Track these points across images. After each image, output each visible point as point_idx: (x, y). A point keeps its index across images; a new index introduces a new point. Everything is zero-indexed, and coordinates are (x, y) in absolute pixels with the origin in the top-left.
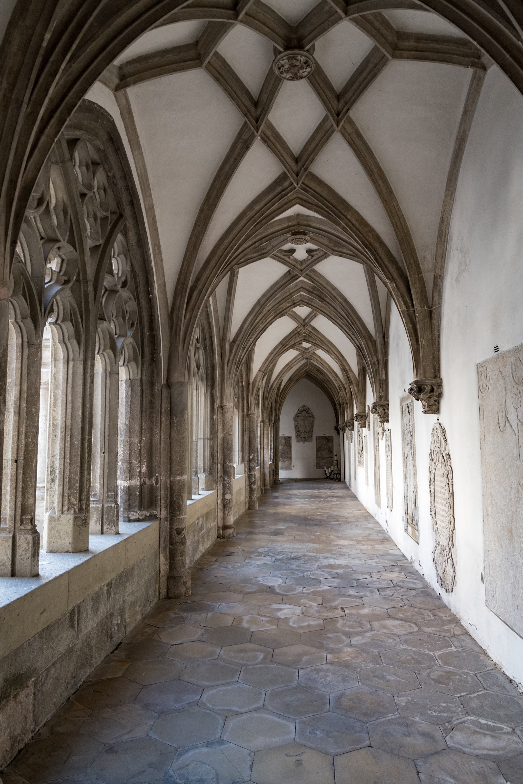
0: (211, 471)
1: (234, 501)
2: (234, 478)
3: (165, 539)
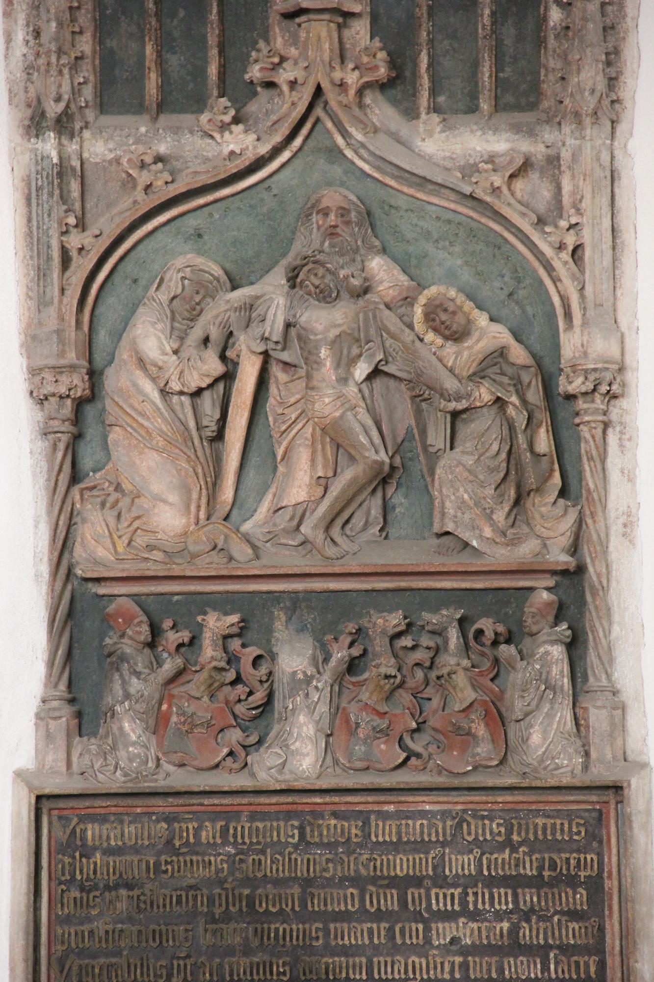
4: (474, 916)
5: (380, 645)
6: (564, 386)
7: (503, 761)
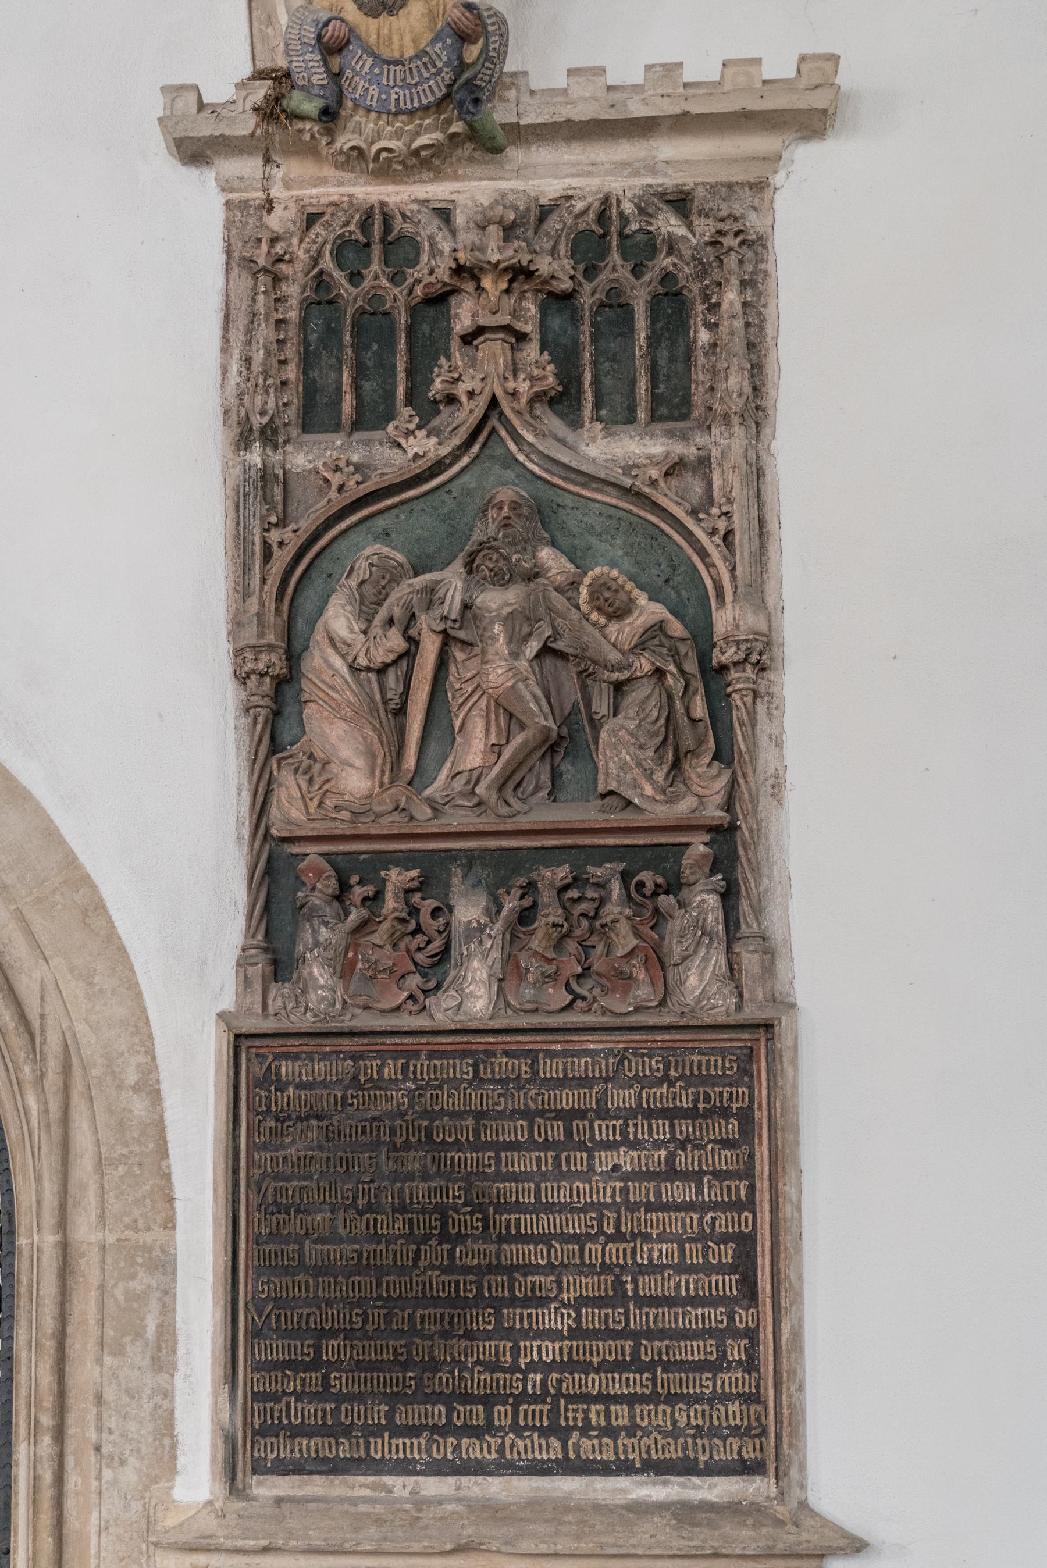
4: (635, 1145)
5: (547, 896)
6: (718, 657)
7: (663, 1003)
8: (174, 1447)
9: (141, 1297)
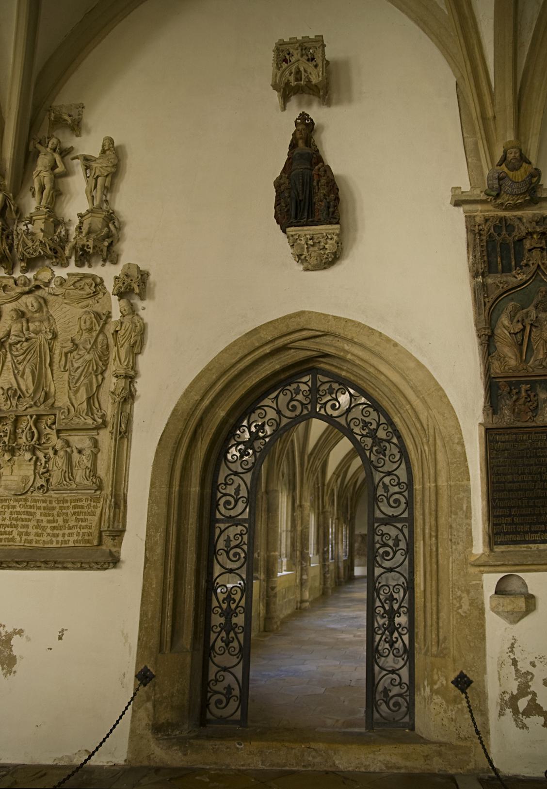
0: (291, 557)
1: (310, 580)
2: (310, 565)
3: (263, 593)
8: (472, 539)
9: (462, 499)
